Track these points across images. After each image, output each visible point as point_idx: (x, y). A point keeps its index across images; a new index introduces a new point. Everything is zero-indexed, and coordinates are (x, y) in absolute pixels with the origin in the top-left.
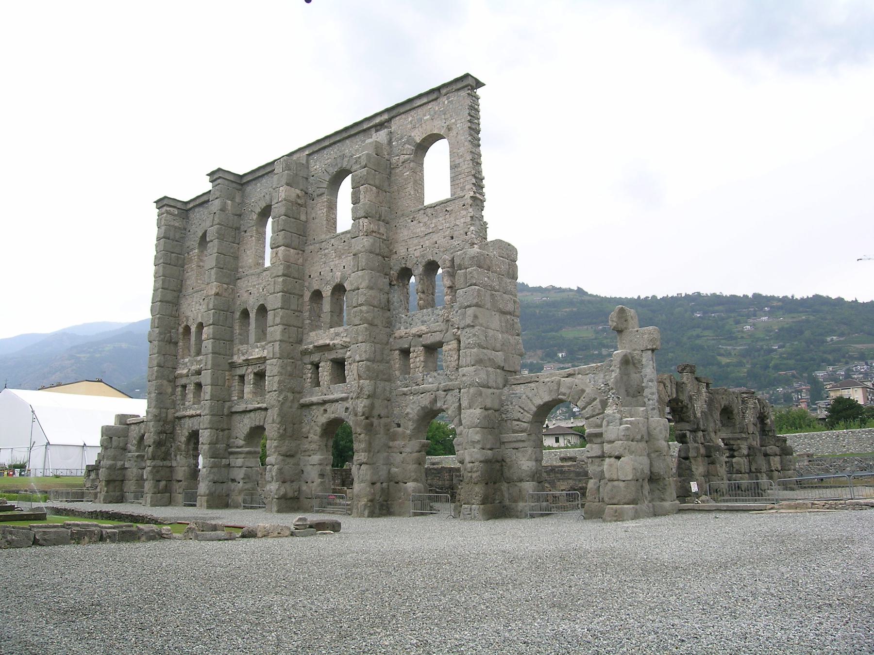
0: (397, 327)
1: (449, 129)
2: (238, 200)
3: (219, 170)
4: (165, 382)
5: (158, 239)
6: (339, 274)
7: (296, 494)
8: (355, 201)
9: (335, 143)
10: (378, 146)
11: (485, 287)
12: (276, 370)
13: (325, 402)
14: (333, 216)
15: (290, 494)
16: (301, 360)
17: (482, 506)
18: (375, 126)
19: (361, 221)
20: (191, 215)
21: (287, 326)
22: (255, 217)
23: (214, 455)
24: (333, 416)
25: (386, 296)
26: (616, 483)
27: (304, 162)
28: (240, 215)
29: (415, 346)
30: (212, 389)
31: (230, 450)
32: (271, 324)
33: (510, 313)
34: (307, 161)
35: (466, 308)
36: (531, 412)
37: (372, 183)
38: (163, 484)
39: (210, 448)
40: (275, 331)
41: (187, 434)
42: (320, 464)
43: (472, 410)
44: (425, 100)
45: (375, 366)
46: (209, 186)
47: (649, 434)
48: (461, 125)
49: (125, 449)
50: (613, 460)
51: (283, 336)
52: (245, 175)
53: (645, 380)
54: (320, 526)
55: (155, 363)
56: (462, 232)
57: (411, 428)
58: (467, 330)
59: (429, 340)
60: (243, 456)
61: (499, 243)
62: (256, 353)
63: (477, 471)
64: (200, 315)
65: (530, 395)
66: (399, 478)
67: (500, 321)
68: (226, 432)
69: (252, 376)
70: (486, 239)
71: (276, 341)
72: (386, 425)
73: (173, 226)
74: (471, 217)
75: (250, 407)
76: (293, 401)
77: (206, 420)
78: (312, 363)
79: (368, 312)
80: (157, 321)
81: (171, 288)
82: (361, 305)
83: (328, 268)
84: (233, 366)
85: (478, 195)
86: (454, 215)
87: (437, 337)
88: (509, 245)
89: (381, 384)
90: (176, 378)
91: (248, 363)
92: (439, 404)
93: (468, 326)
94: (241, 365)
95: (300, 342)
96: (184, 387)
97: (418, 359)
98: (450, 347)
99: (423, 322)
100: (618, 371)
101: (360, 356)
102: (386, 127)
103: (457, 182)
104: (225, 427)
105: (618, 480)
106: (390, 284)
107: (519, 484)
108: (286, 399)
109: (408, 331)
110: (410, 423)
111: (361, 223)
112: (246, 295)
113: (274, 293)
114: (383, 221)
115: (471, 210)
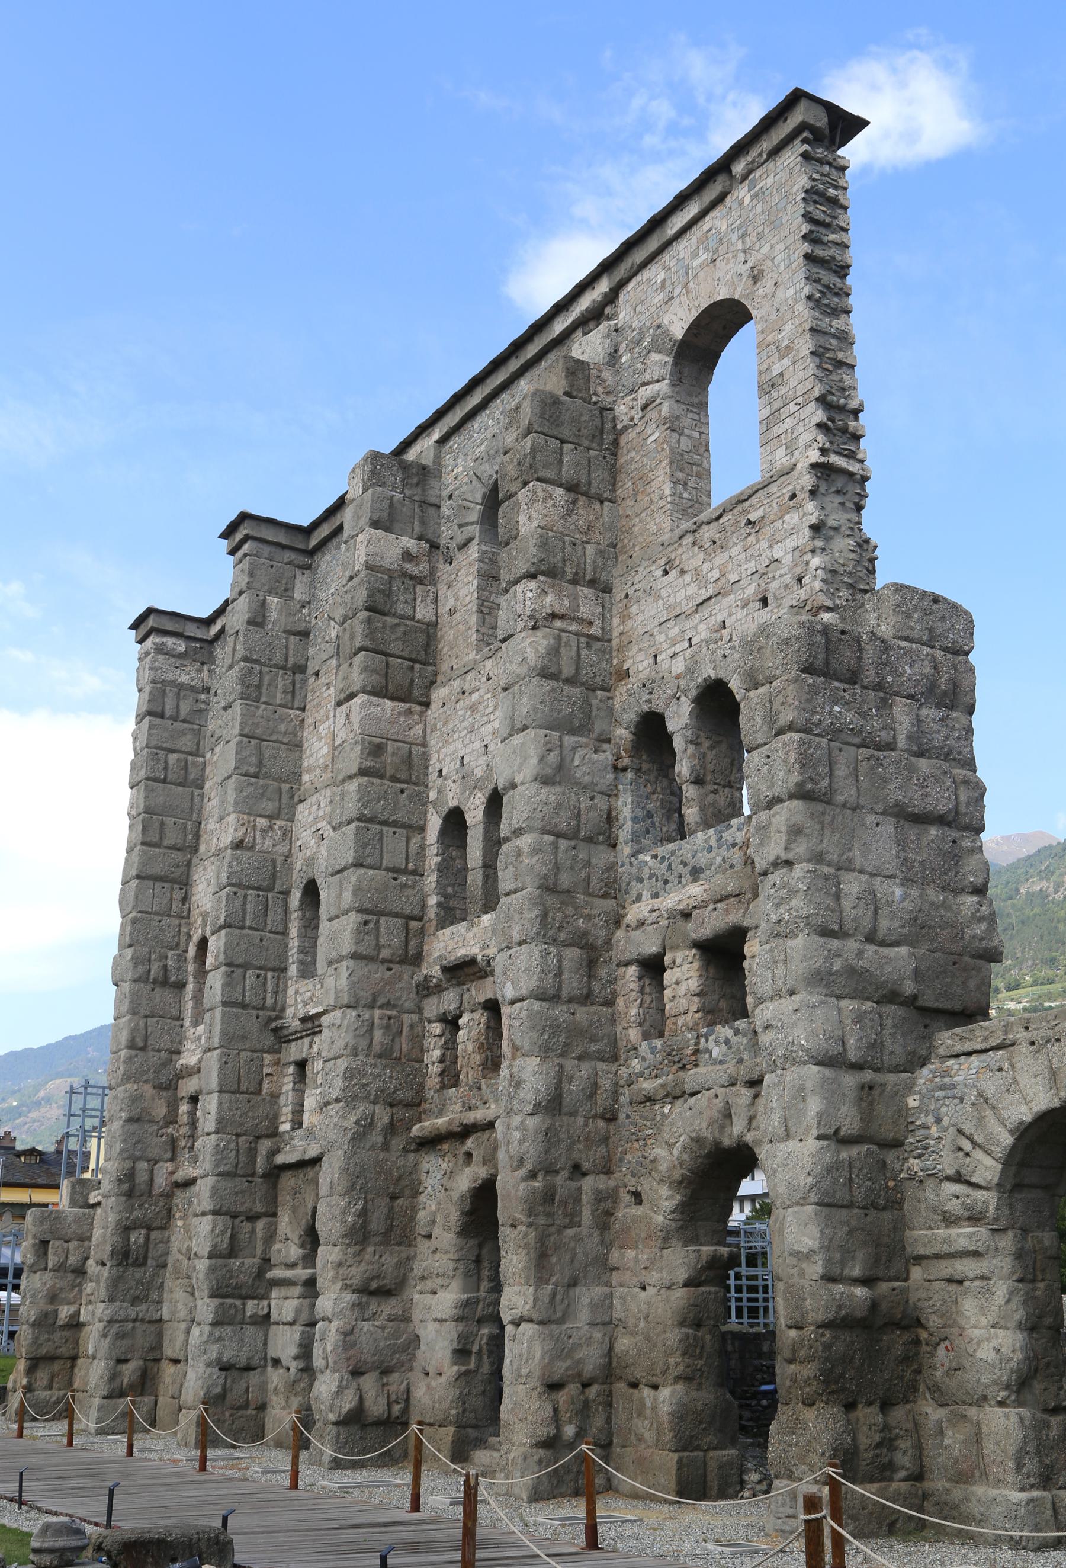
0: (634, 893)
2: (299, 593)
3: (244, 517)
4: (148, 1090)
7: (397, 1409)
15: (376, 1407)
16: (420, 1010)
21: (371, 913)
25: (601, 802)
27: (428, 461)
29: (675, 948)
30: (220, 1104)
31: (270, 1275)
33: (941, 820)
34: (438, 459)
36: (998, 1152)
37: (550, 474)
38: (129, 1371)
39: (212, 1269)
43: (793, 1145)
44: (692, 209)
45: (560, 1012)
51: (358, 942)
56: (788, 579)
57: (668, 1205)
58: (776, 877)
59: (711, 923)
63: (809, 1360)
65: (990, 1088)
66: (639, 1373)
67: (902, 844)
68: (260, 1224)
72: (600, 1197)
73: (173, 683)
76: (391, 1129)
81: (166, 843)
83: (478, 745)
85: (834, 459)
86: (767, 531)
88: (936, 599)
90: (179, 1076)
92: (738, 1127)
95: (417, 959)
97: (682, 989)
99: (696, 873)
102: (609, 319)
103: (777, 430)
104: (259, 1208)
106: (615, 768)
107: (972, 1412)
108: (365, 1127)
110: (664, 1191)
111: (520, 595)
114: (592, 583)
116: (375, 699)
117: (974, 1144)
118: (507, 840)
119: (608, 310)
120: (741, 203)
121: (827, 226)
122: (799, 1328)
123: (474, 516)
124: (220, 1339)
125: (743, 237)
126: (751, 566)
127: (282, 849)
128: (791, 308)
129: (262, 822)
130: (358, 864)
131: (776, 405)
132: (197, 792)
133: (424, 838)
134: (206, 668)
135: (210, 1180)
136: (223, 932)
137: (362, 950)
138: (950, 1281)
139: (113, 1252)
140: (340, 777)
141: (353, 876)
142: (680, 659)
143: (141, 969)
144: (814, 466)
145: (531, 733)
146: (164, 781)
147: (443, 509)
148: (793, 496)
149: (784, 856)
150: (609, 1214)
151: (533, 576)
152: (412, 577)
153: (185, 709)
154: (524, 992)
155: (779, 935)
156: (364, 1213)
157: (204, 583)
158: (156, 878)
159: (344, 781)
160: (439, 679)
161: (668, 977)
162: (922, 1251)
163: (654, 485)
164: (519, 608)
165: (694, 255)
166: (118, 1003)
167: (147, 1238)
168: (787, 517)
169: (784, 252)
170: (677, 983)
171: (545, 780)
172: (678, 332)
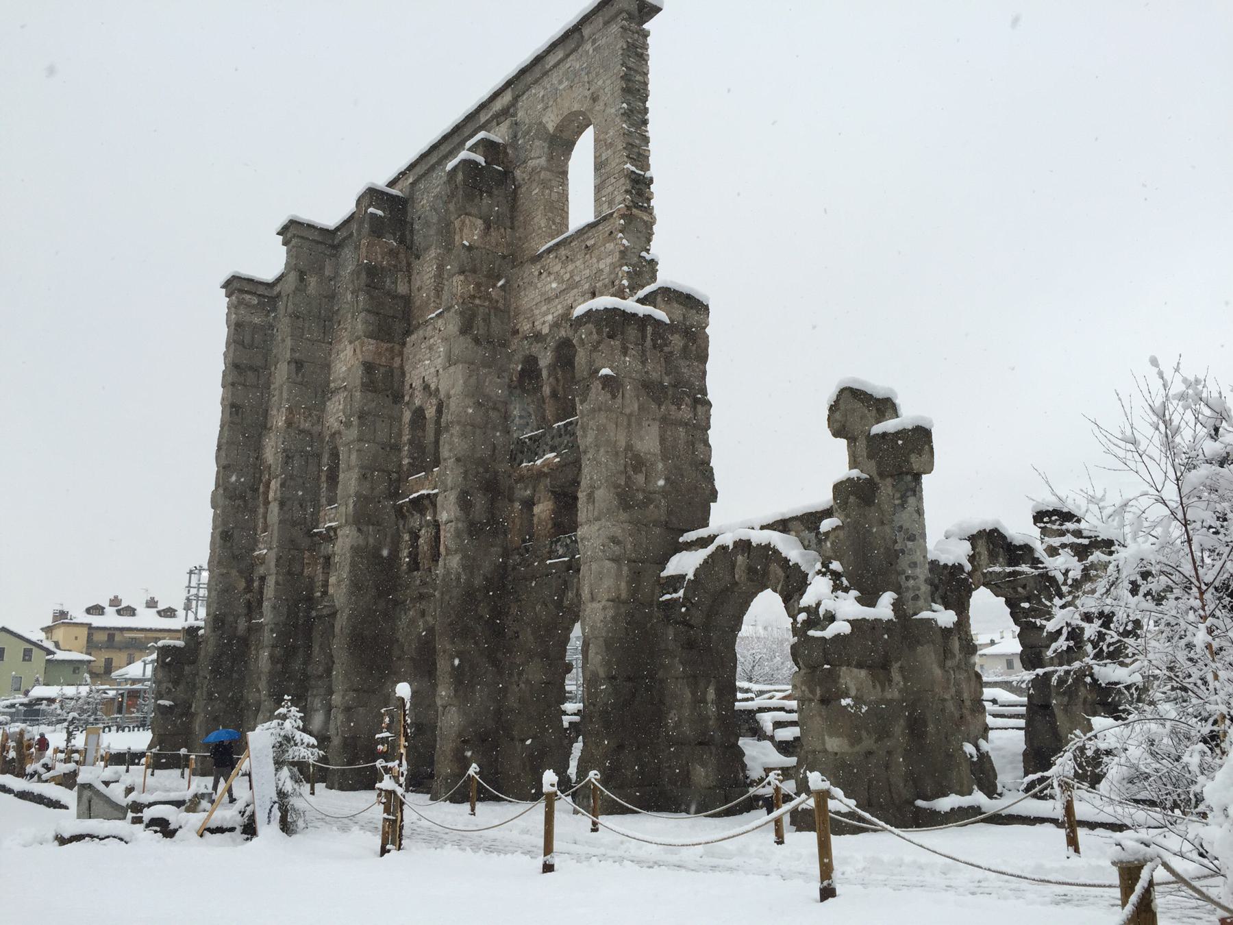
2: (328, 272)
4: (234, 572)
10: (488, 147)
44: (560, 54)
83: (433, 370)
86: (596, 252)
106: (509, 386)
119: (511, 110)
120: (587, 52)
121: (636, 71)
125: (587, 74)
127: (317, 428)
128: (613, 121)
157: (269, 261)
164: (454, 290)
165: (560, 82)
169: (609, 85)
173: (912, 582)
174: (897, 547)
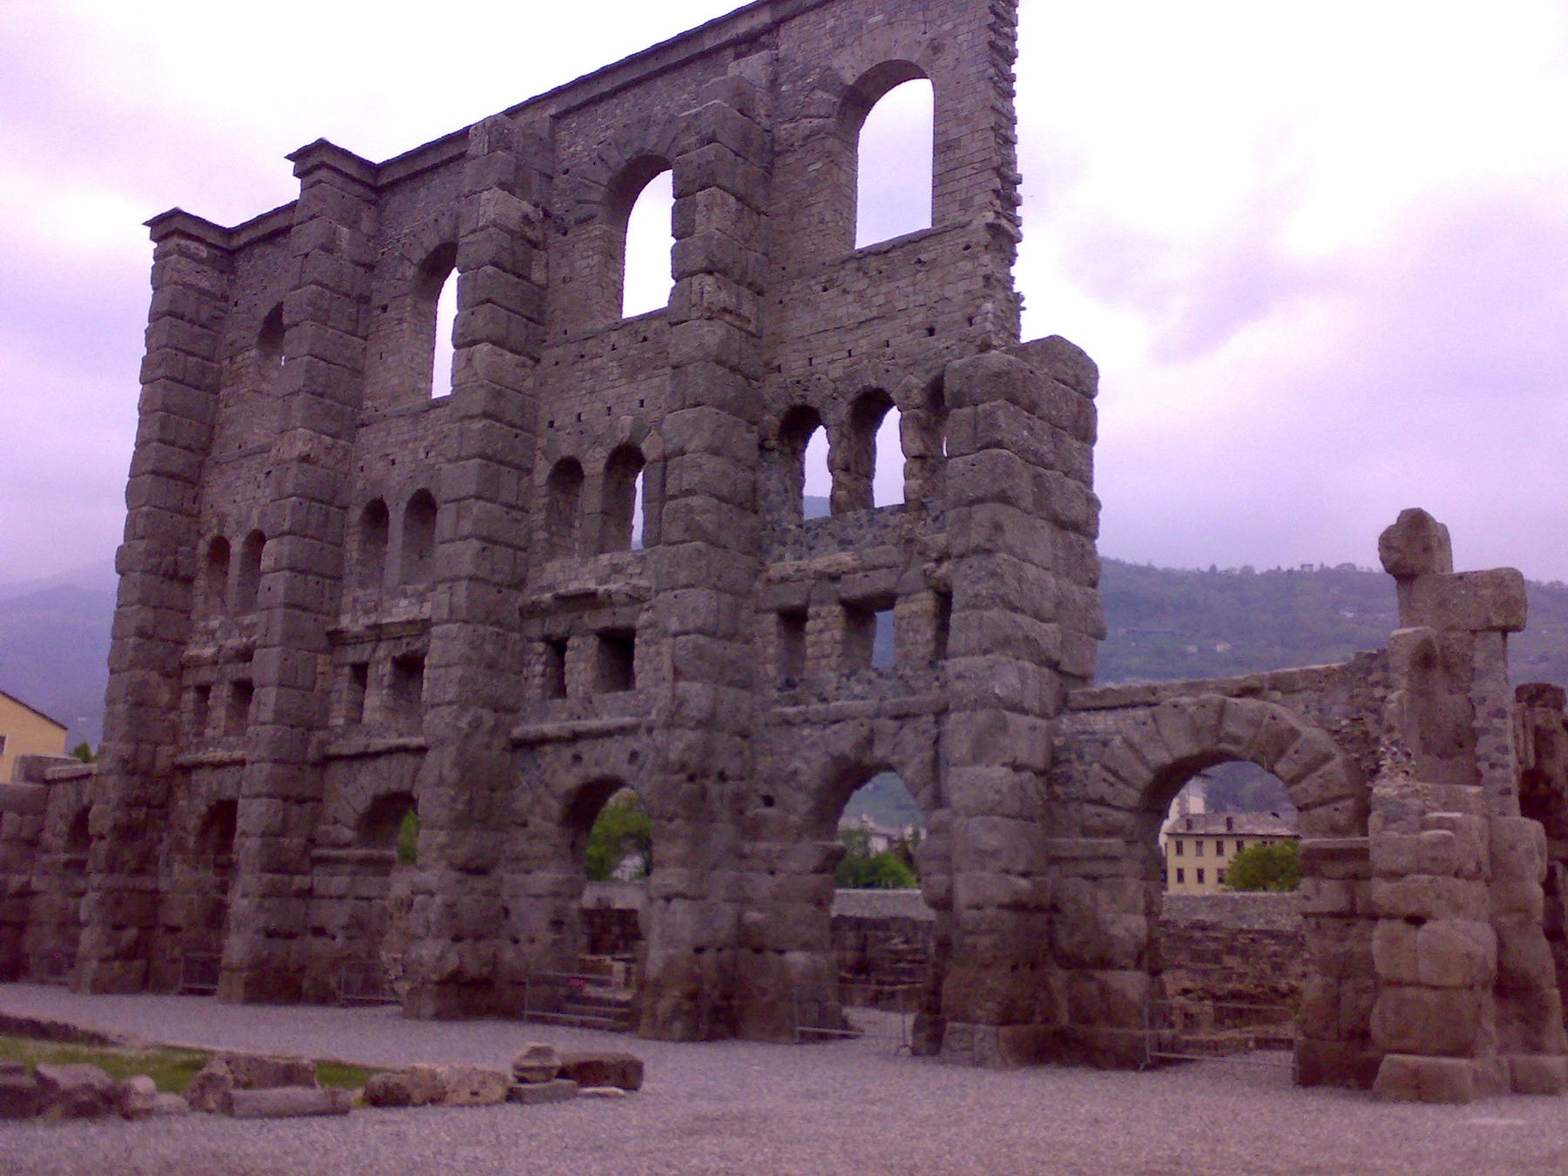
0: (775, 553)
1: (936, 48)
2: (367, 226)
4: (154, 677)
5: (154, 316)
6: (627, 420)
8: (681, 228)
9: (626, 87)
11: (1023, 452)
12: (458, 649)
13: (576, 737)
14: (615, 277)
15: (473, 969)
17: (1005, 1030)
18: (735, 43)
19: (696, 280)
20: (243, 266)
22: (411, 272)
23: (276, 865)
24: (595, 772)
25: (749, 475)
26: (1409, 992)
27: (545, 135)
28: (370, 267)
29: (822, 603)
30: (278, 698)
31: (317, 852)
32: (448, 534)
34: (552, 134)
35: (971, 503)
36: (1140, 784)
37: (727, 184)
40: (457, 551)
41: (204, 809)
42: (556, 894)
43: (979, 769)
46: (289, 189)
47: (1493, 859)
48: (968, 38)
49: (33, 843)
50: (1399, 926)
51: (478, 567)
52: (388, 164)
53: (1481, 712)
54: (586, 1073)
55: (131, 626)
56: (958, 316)
58: (975, 560)
59: (858, 588)
60: (348, 868)
61: (1056, 350)
62: (402, 610)
64: (255, 512)
65: (1136, 738)
67: (1054, 544)
68: (308, 807)
69: (387, 668)
70: (1017, 337)
71: (457, 579)
74: (987, 278)
75: (379, 744)
76: (493, 731)
77: (260, 773)
78: (547, 639)
79: (705, 511)
80: (141, 522)
82: (688, 493)
83: (599, 405)
84: (336, 639)
85: (1004, 222)
87: (881, 582)
89: (730, 694)
90: (183, 667)
91: (378, 632)
92: (880, 752)
93: (977, 550)
94: (359, 639)
95: (519, 584)
96: (204, 690)
97: (826, 636)
98: (913, 607)
100: (1404, 682)
101: (682, 620)
102: (764, 47)
103: (951, 187)
104: (308, 793)
105: (1417, 984)
106: (761, 447)
107: (1098, 974)
109: (803, 563)
111: (696, 287)
112: (380, 465)
113: (458, 458)
114: (750, 285)
115: (986, 258)
116: (498, 349)
117: (1120, 778)
118: (674, 497)
122: (978, 907)
123: (597, 197)
124: (269, 909)
126: (921, 298)
129: (327, 440)
130: (478, 497)
131: (952, 166)
132: (212, 397)
133: (532, 480)
134: (225, 277)
135: (267, 767)
136: (287, 539)
137: (480, 574)
138: (1086, 877)
139: (115, 827)
140: (461, 414)
141: (477, 507)
142: (839, 364)
143: (154, 561)
144: (989, 226)
145: (706, 409)
146: (181, 382)
147: (556, 181)
148: (967, 248)
149: (988, 545)
150: (741, 812)
151: (710, 273)
152: (529, 241)
153: (205, 315)
154: (690, 627)
155: (975, 607)
156: (470, 802)
158: (172, 476)
159: (462, 419)
160: (550, 339)
161: (809, 625)
162: (1063, 854)
163: (814, 210)
165: (870, 13)
166: (121, 592)
167: (147, 814)
168: (961, 264)
170: (821, 631)
171: (716, 452)
172: (849, 78)
173: (1498, 773)
174: (1475, 724)
